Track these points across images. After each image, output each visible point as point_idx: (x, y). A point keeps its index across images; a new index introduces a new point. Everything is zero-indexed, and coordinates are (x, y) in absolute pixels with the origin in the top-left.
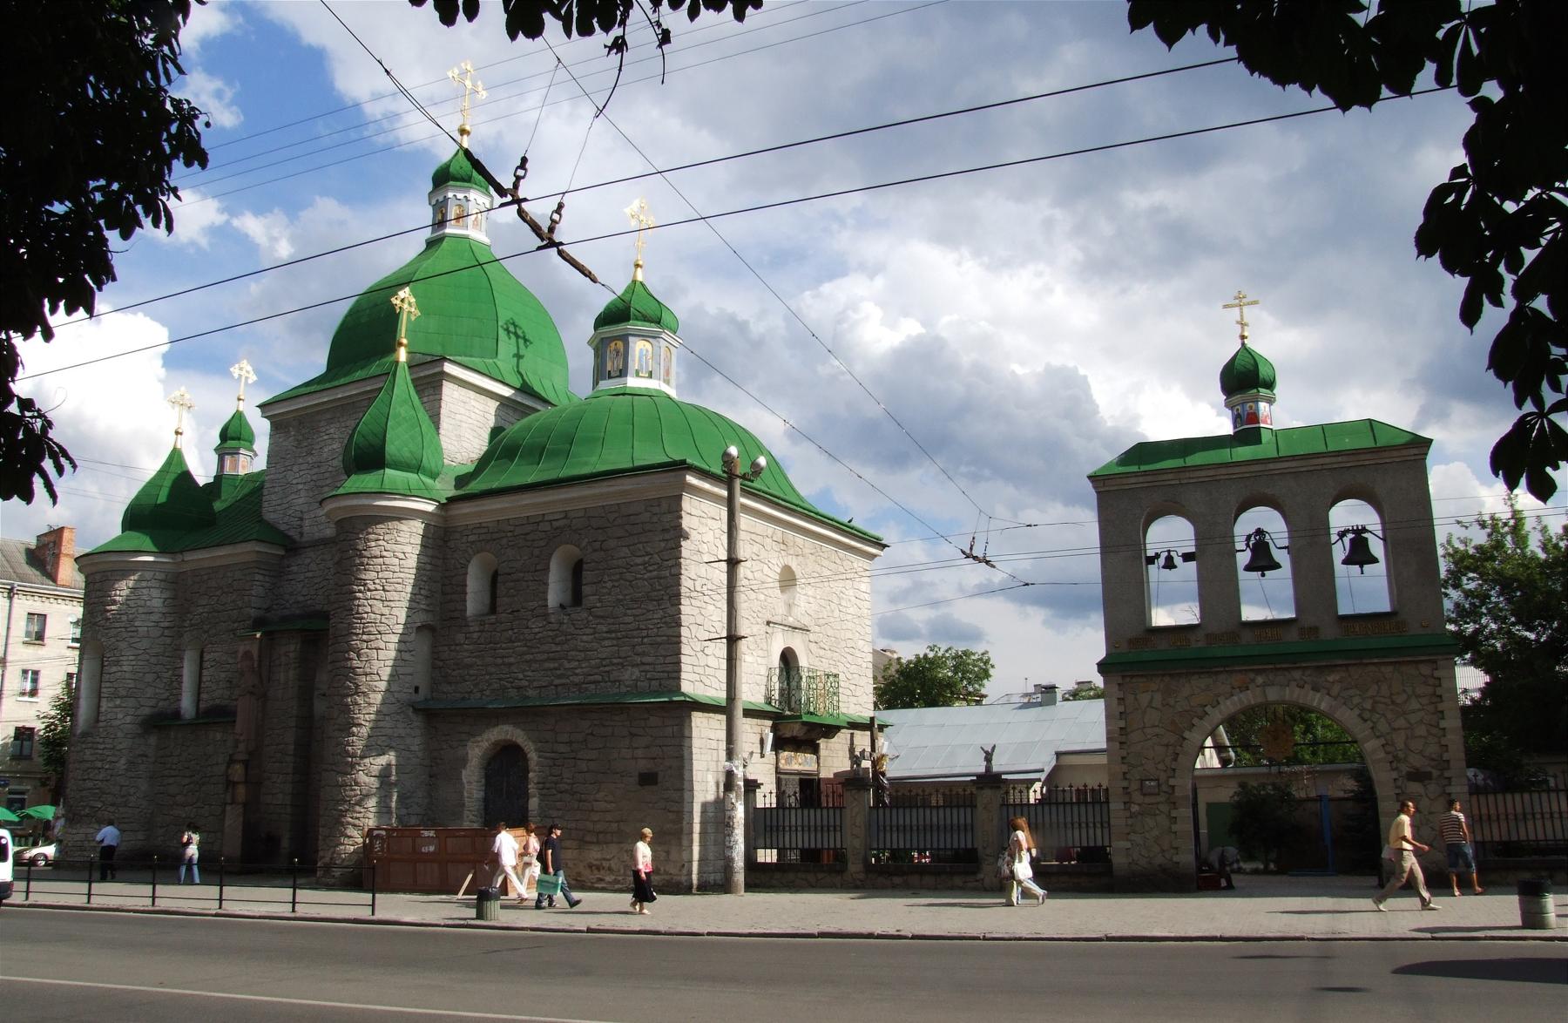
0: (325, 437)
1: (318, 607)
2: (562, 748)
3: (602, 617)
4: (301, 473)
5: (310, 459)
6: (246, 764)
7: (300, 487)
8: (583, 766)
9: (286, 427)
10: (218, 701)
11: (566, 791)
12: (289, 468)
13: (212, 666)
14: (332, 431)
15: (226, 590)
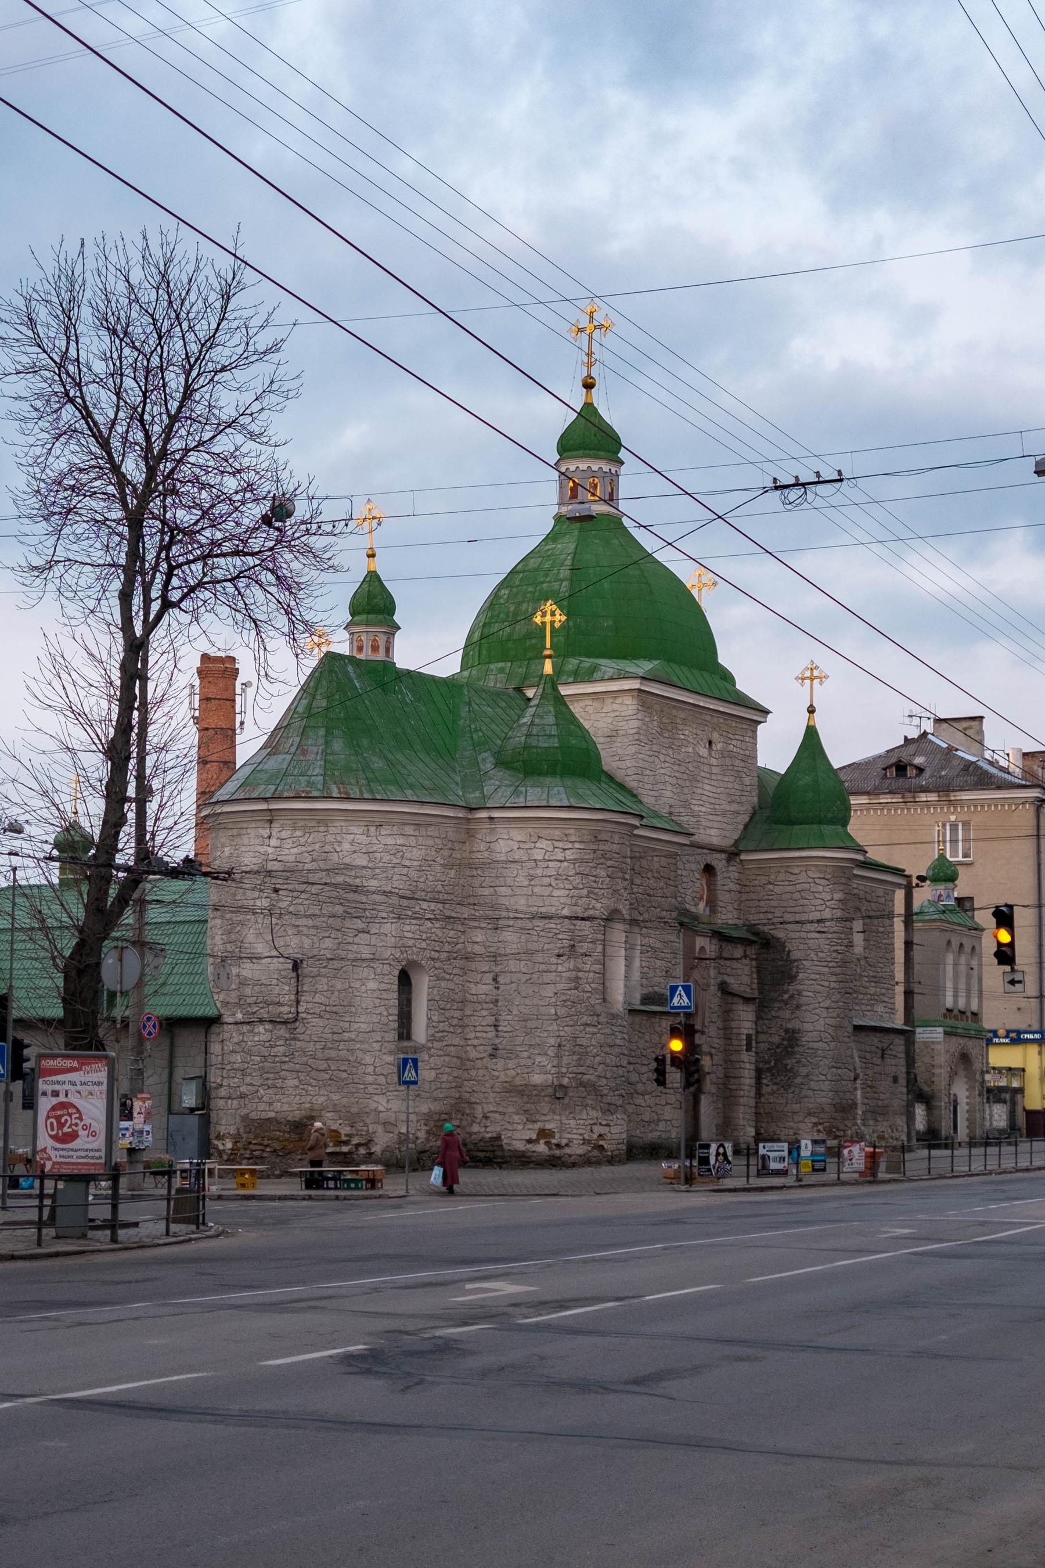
0: (682, 737)
1: (688, 906)
2: (868, 1056)
3: (870, 965)
4: (667, 765)
5: (670, 752)
6: (711, 1055)
7: (667, 779)
8: (877, 1069)
9: (648, 708)
10: (656, 989)
11: (870, 1086)
12: (657, 754)
13: (648, 952)
14: (686, 732)
15: (656, 875)
